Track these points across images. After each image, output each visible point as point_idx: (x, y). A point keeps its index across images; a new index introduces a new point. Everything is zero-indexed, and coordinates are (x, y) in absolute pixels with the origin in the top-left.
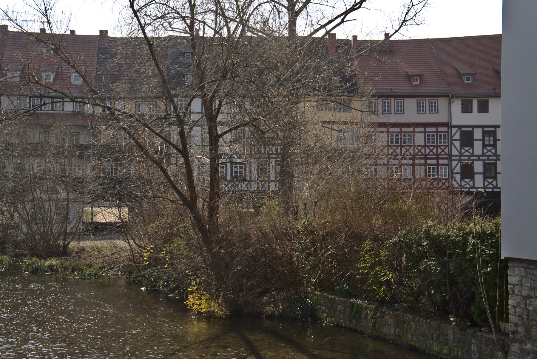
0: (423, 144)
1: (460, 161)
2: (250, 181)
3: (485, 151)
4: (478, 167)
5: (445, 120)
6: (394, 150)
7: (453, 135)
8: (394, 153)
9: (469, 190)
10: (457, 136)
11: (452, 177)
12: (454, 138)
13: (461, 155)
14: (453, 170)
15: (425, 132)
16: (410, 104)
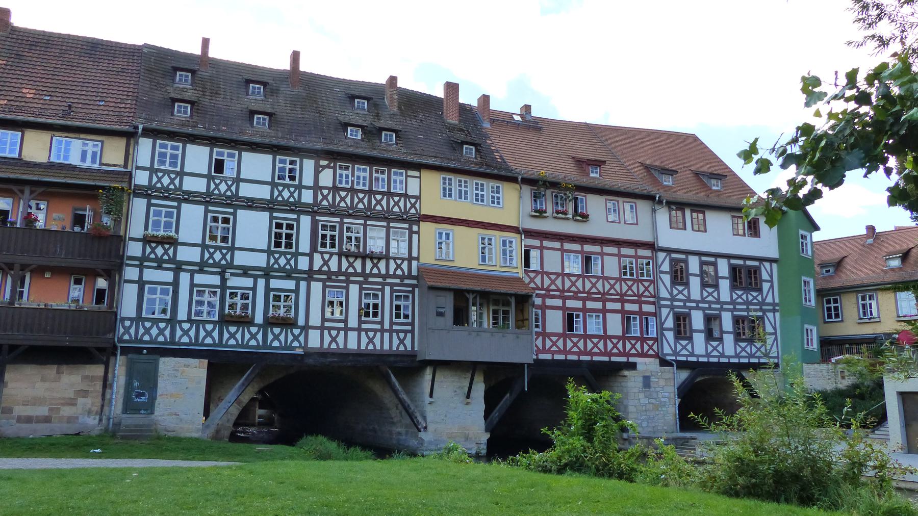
0: (618, 276)
1: (672, 307)
2: (306, 328)
3: (705, 294)
4: (697, 320)
5: (647, 238)
6: (574, 284)
7: (660, 263)
8: (573, 289)
9: (687, 359)
10: (666, 267)
11: (663, 334)
12: (662, 269)
13: (673, 299)
14: (663, 324)
15: (619, 256)
16: (594, 205)
